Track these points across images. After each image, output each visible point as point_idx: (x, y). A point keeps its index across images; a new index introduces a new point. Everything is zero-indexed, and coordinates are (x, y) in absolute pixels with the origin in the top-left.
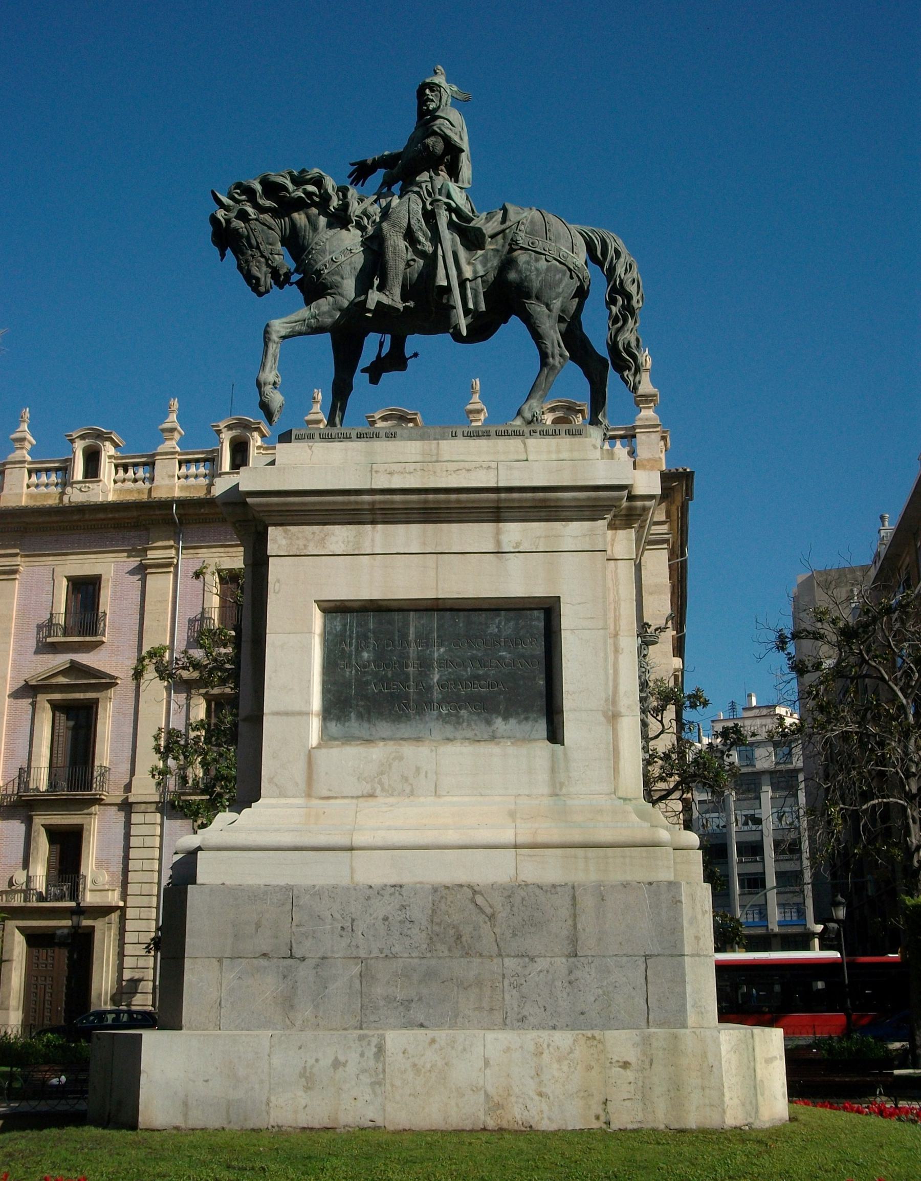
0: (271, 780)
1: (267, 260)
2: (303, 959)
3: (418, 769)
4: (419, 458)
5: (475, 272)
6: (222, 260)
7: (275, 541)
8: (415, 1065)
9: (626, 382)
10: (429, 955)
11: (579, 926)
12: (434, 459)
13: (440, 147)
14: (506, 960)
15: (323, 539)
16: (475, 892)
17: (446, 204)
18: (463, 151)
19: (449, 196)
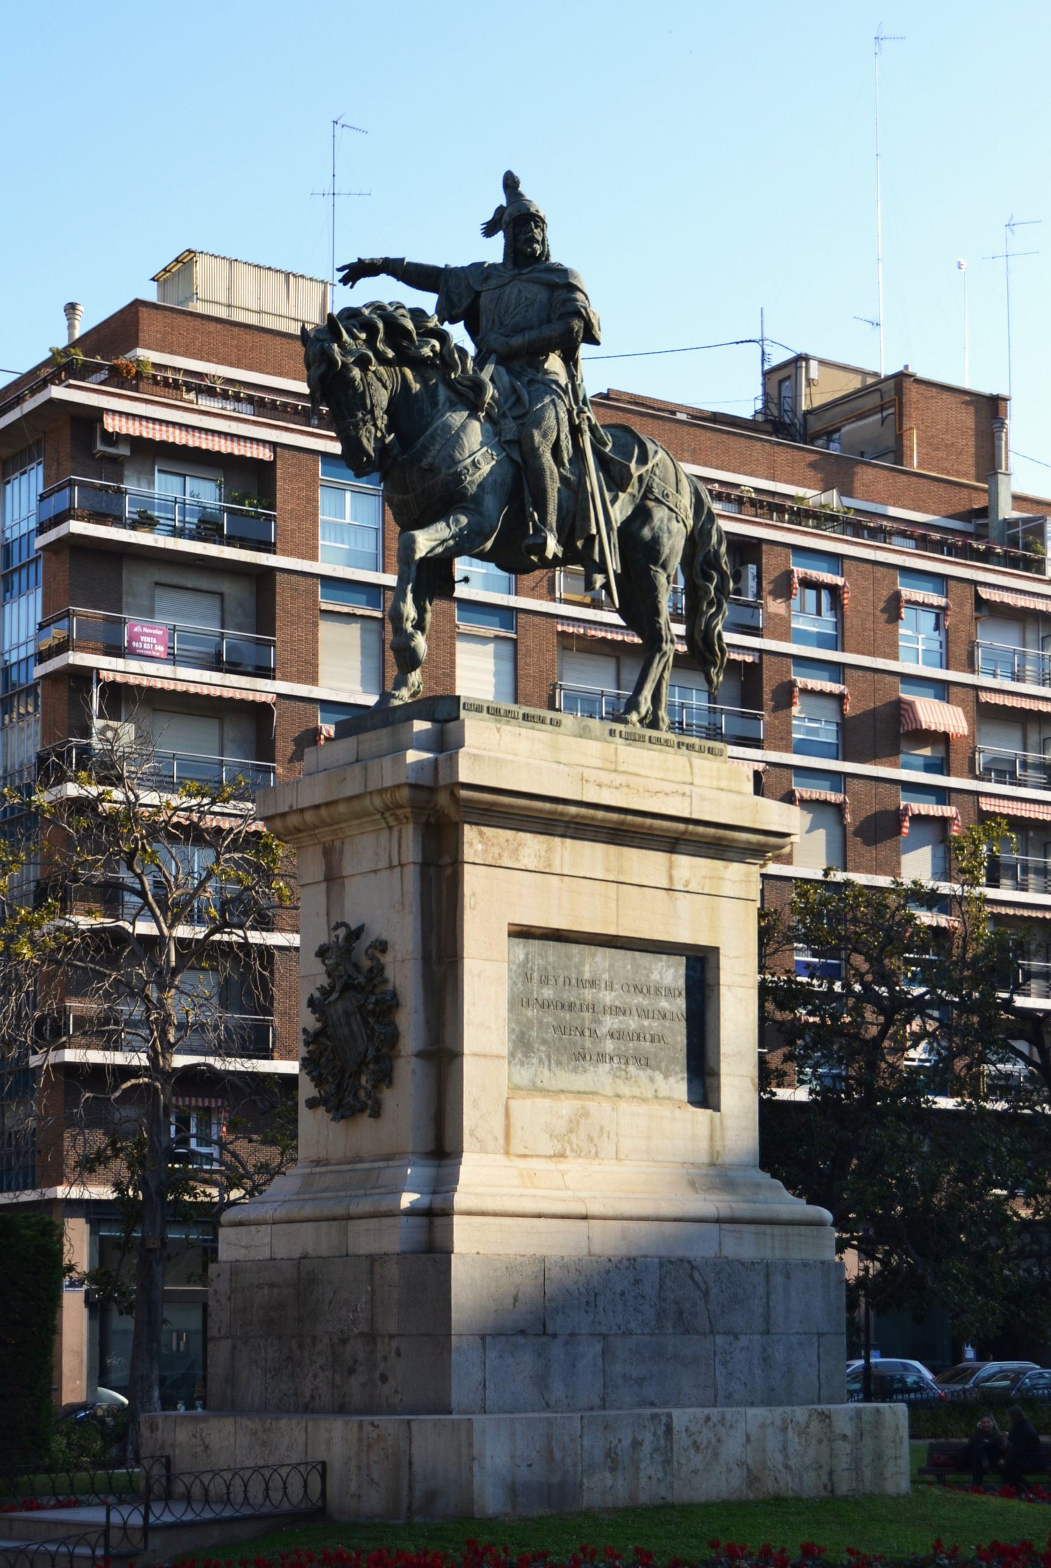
0: (472, 1133)
2: (555, 1336)
3: (602, 1129)
4: (599, 763)
7: (471, 844)
8: (695, 1443)
10: (657, 1331)
11: (771, 1304)
12: (613, 767)
14: (717, 1337)
15: (517, 849)
16: (693, 1268)
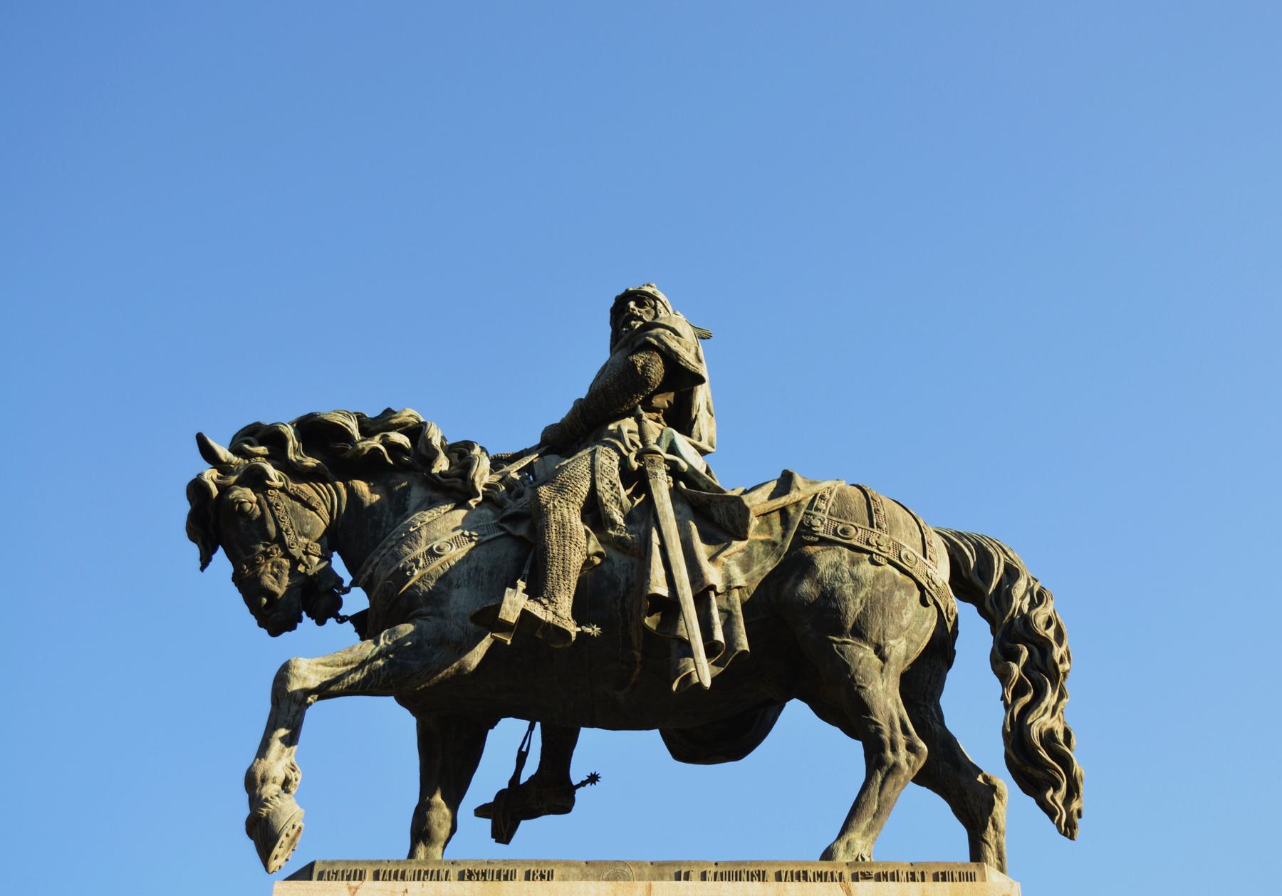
1: (295, 562)
5: (728, 580)
6: (202, 569)
9: (1051, 813)
13: (657, 370)
17: (666, 461)
18: (701, 380)
19: (673, 449)
